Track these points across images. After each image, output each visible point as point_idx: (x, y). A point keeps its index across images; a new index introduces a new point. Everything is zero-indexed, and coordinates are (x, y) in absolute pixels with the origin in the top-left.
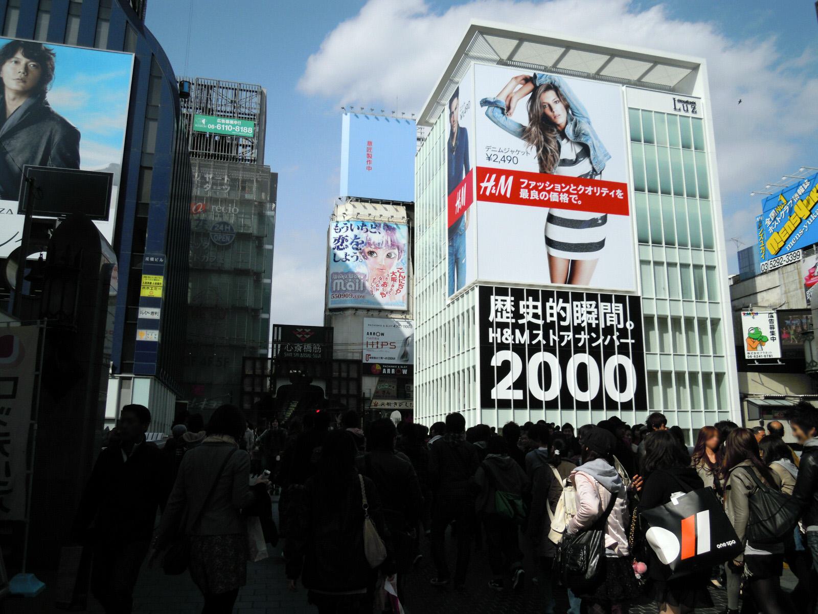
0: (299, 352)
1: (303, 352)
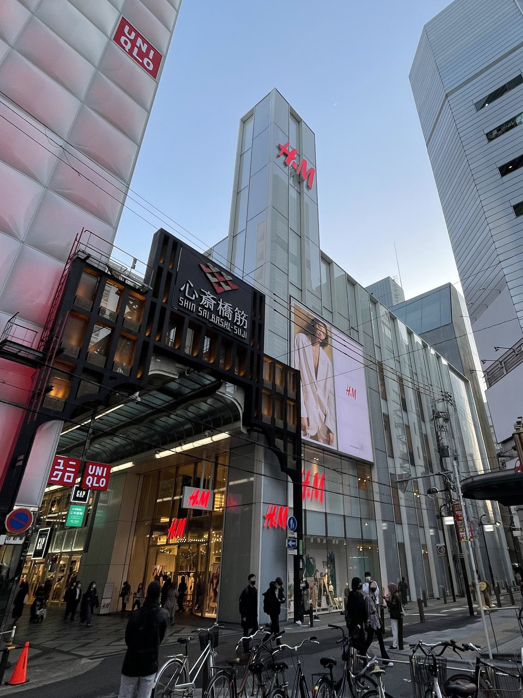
0: (209, 309)
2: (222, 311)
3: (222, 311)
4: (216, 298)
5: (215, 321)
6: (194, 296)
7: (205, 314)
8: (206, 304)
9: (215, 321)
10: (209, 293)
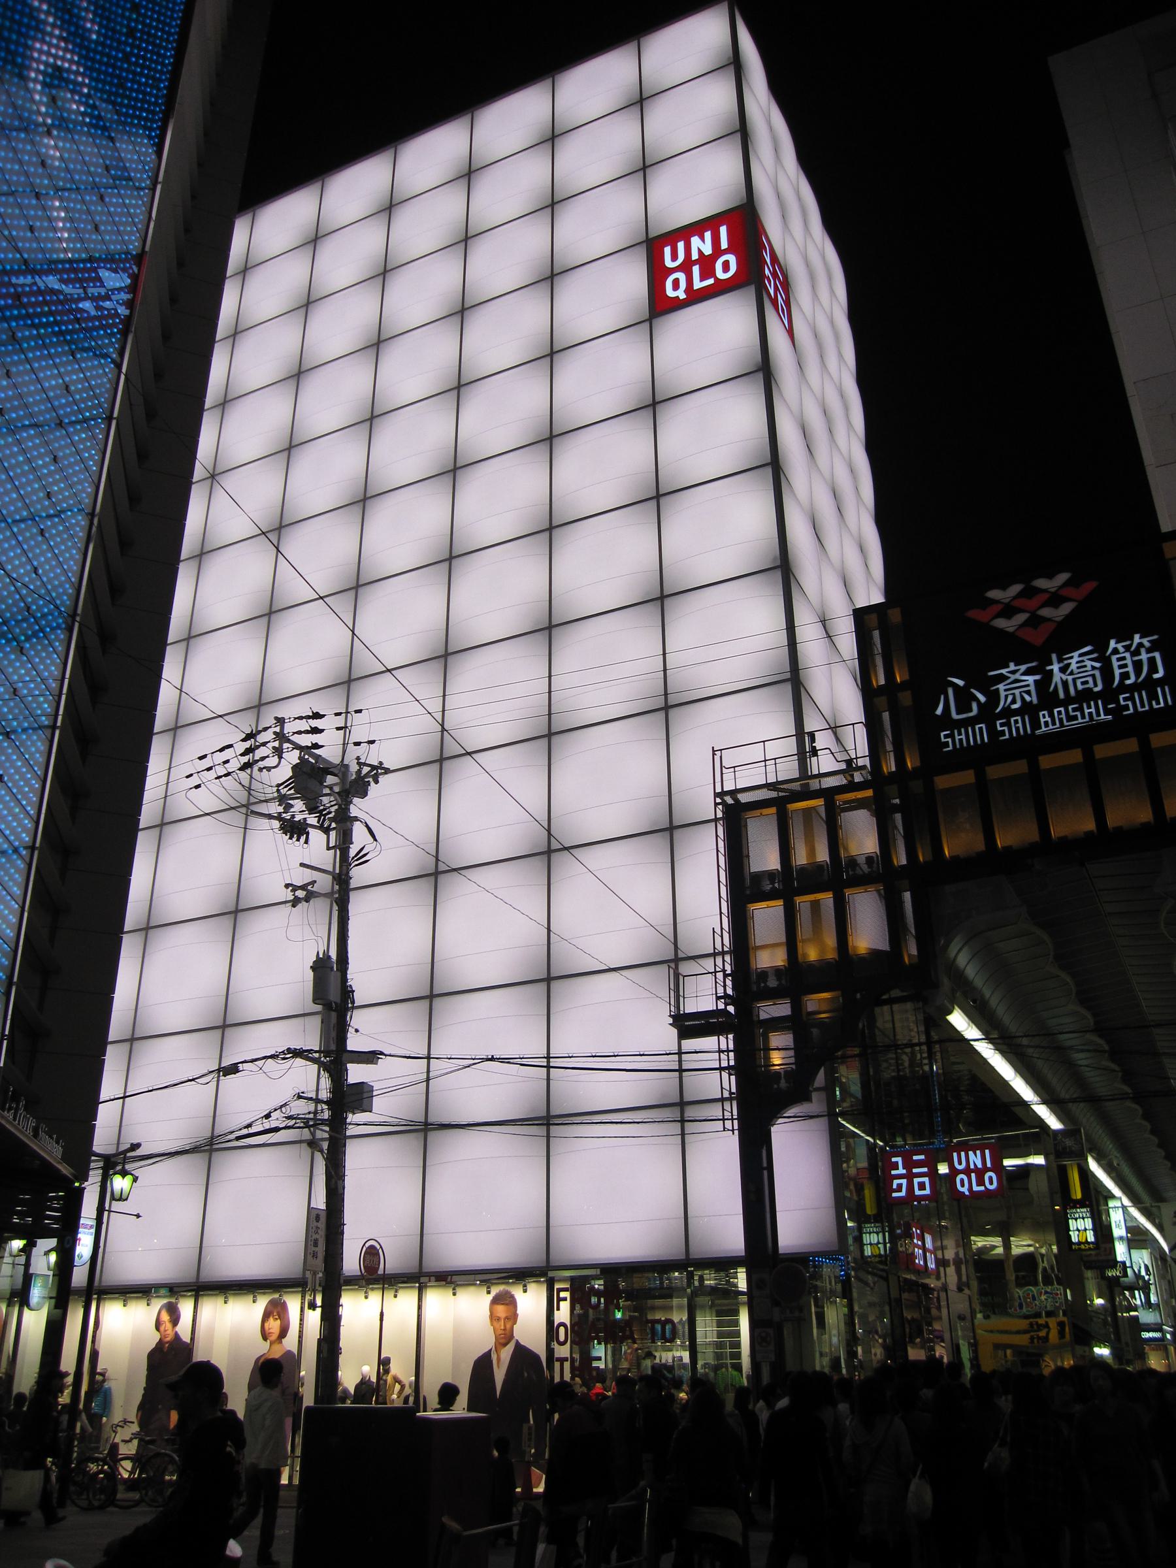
0: (1026, 708)
1: (1047, 698)
2: (1065, 684)
3: (1065, 684)
4: (1034, 664)
5: (1054, 723)
6: (974, 706)
7: (1017, 729)
8: (1014, 701)
9: (1054, 723)
10: (1012, 667)
